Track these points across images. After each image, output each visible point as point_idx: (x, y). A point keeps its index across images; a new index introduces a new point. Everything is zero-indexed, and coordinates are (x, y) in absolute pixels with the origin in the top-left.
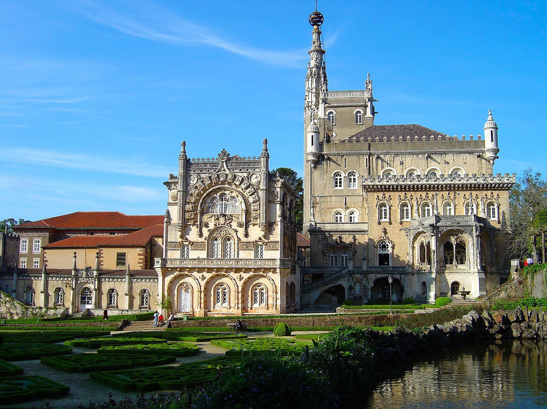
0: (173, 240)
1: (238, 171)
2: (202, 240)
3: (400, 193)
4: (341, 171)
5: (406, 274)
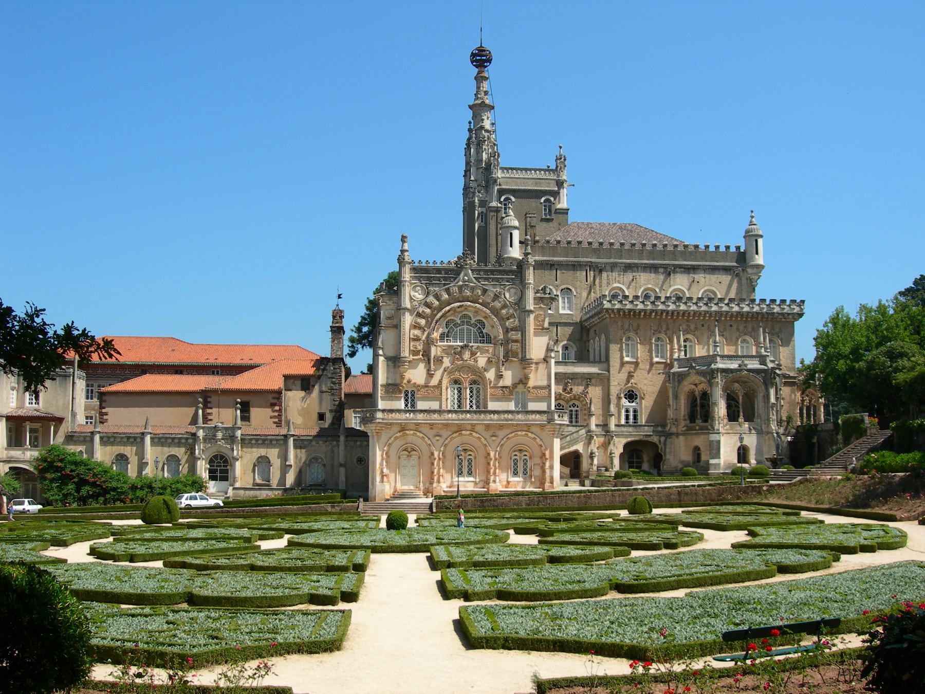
0: (390, 382)
2: (434, 382)
5: (669, 435)
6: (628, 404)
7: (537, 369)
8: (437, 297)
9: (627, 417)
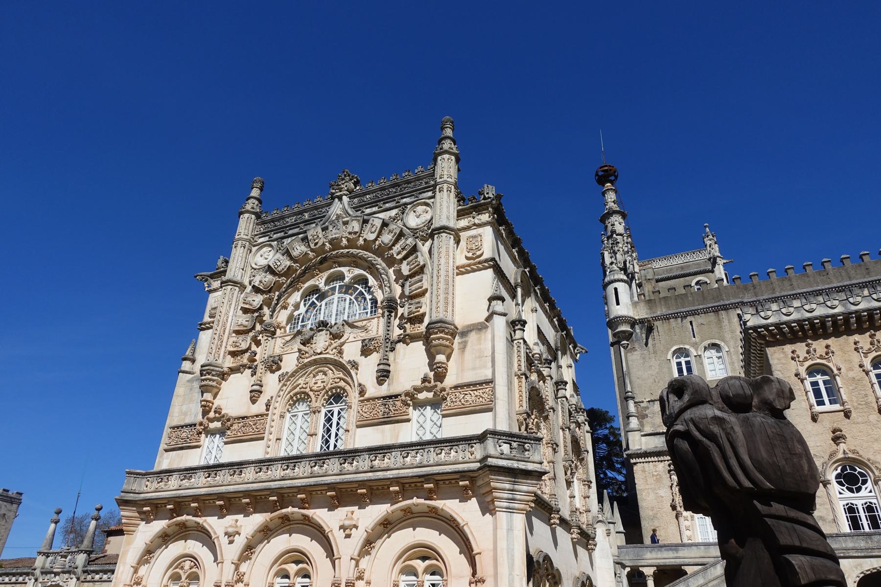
1: (375, 209)
2: (259, 407)
3: (857, 337)
4: (687, 347)
6: (848, 494)
7: (463, 348)
8: (287, 253)
9: (855, 523)
